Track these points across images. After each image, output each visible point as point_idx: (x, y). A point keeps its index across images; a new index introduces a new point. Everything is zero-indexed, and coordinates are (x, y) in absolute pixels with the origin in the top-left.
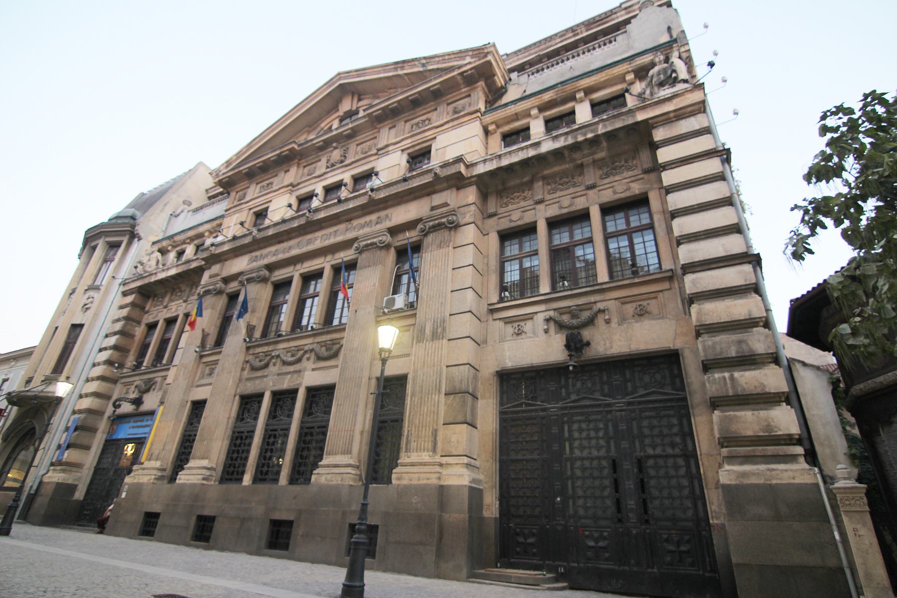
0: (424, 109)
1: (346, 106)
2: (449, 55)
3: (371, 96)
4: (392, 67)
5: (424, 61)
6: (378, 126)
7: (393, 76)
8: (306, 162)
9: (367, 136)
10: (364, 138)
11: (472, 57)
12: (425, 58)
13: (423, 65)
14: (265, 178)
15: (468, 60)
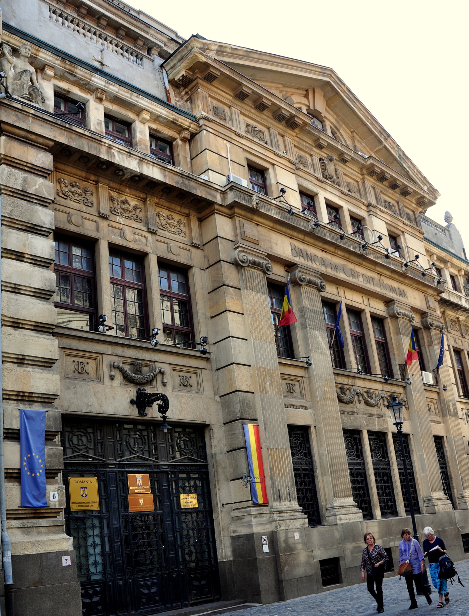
0: (393, 194)
1: (320, 106)
2: (417, 170)
3: (335, 117)
4: (380, 129)
5: (402, 155)
6: (366, 176)
7: (376, 136)
8: (298, 142)
9: (352, 174)
10: (350, 172)
11: (428, 189)
12: (404, 153)
13: (400, 156)
14: (254, 117)
15: (425, 188)
